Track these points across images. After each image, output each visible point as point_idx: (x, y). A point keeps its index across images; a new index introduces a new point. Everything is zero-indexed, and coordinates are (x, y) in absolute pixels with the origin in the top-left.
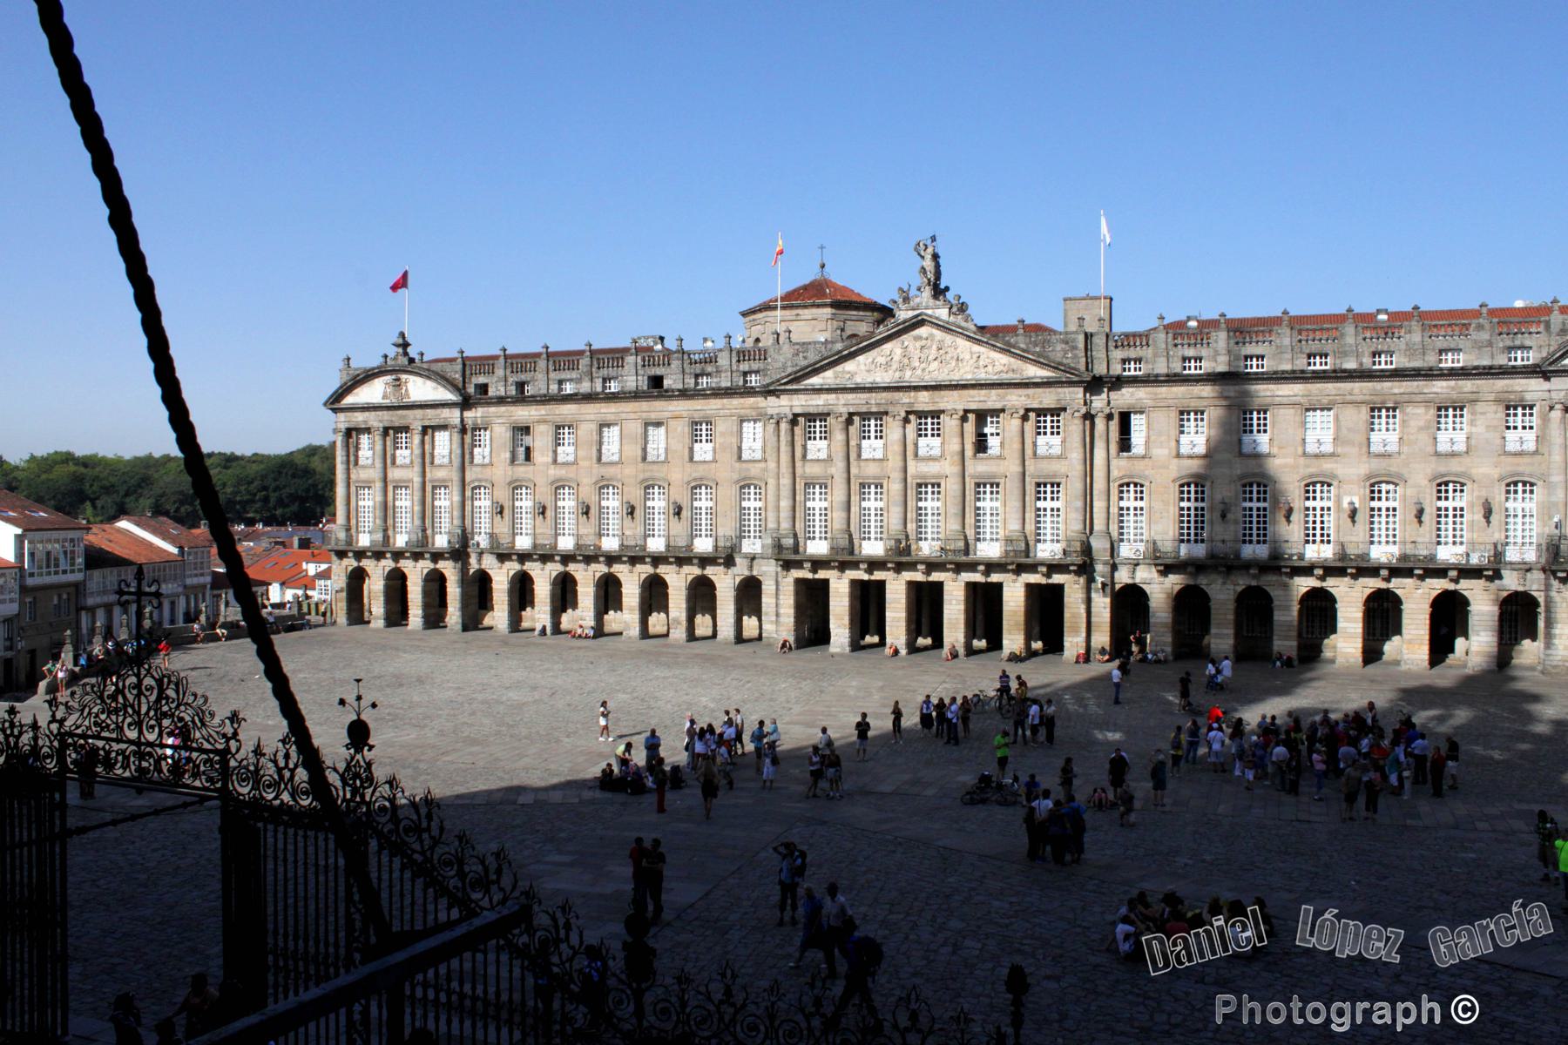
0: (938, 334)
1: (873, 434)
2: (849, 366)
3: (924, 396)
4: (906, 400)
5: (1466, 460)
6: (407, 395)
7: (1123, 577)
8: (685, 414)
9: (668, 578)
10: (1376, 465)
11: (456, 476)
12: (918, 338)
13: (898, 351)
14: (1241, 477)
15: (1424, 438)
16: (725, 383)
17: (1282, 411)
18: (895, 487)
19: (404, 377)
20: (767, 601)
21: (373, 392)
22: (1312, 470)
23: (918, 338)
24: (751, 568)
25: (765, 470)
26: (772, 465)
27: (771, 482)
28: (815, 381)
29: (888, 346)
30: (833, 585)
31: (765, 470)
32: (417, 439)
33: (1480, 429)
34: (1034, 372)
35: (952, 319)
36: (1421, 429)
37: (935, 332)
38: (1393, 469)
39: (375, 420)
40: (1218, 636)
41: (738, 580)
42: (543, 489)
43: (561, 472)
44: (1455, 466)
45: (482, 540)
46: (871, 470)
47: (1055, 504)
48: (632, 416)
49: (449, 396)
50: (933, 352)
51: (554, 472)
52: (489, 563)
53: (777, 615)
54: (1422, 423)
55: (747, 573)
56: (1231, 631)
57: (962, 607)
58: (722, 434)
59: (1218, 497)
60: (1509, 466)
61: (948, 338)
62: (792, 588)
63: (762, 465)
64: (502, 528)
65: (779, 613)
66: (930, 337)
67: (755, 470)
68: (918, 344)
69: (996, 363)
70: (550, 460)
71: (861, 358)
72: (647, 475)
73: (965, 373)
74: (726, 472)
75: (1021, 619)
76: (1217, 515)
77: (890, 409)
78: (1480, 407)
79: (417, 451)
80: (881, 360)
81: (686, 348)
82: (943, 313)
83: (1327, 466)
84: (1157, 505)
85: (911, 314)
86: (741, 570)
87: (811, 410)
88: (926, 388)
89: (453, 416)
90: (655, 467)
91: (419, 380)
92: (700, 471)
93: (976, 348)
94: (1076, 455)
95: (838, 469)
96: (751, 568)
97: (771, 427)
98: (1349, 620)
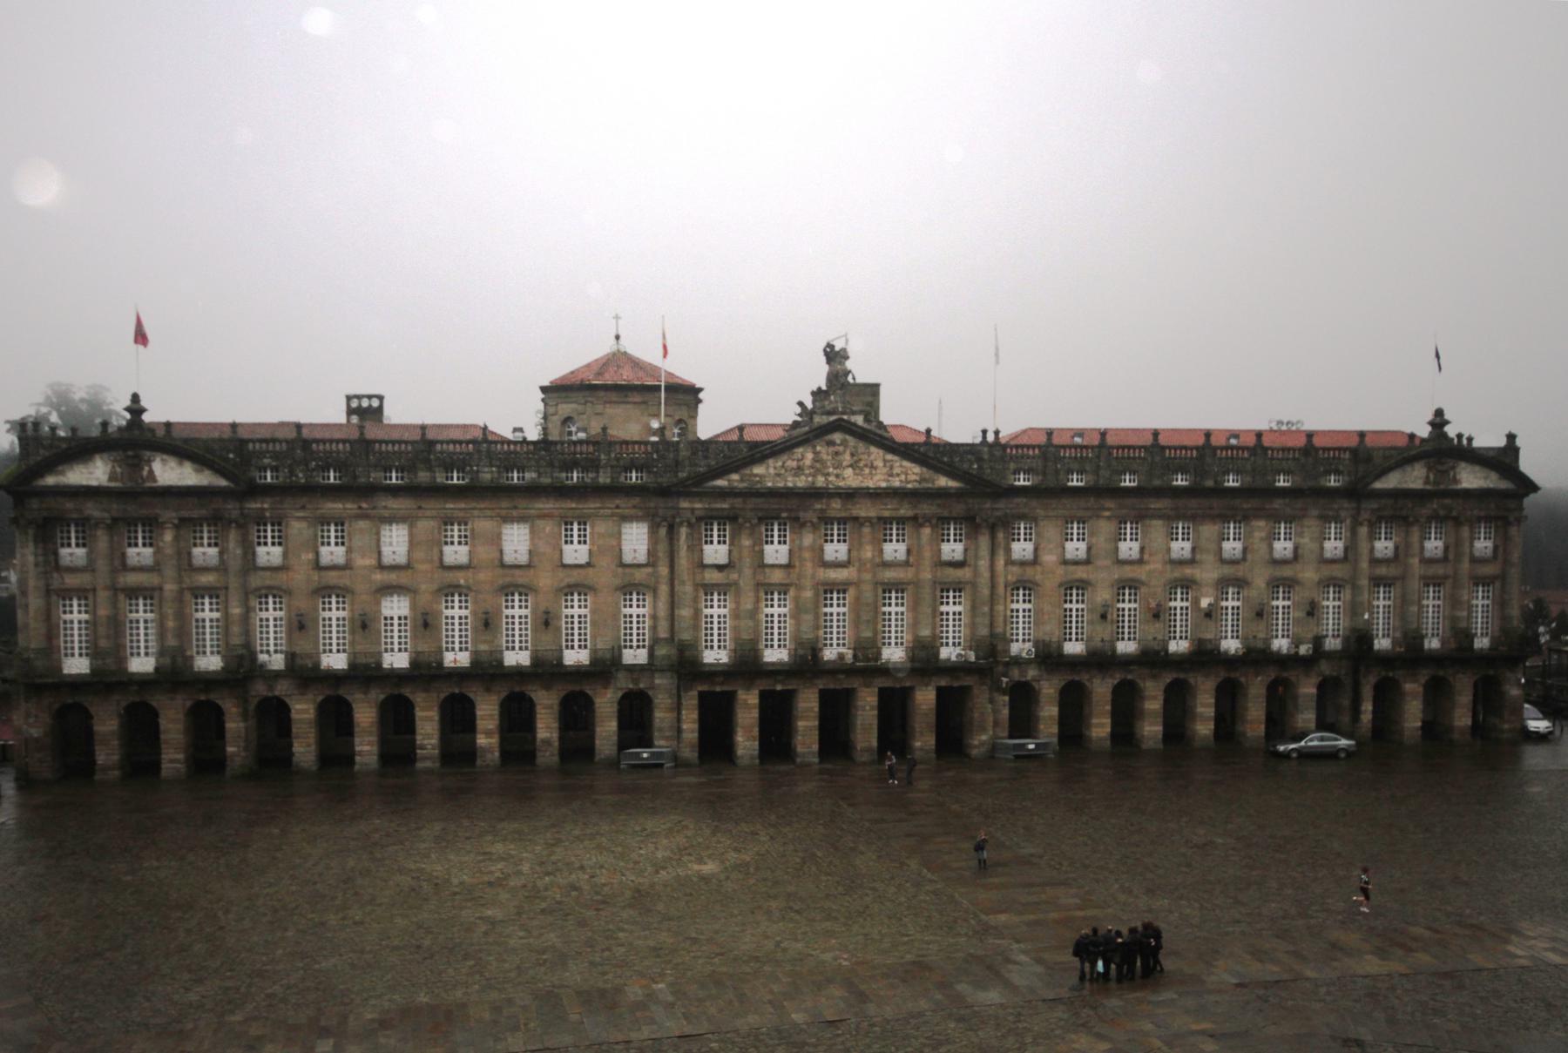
0: (851, 440)
1: (776, 539)
2: (758, 470)
3: (836, 504)
4: (818, 506)
5: (1298, 566)
6: (155, 480)
7: (1016, 674)
8: (556, 512)
9: (533, 695)
10: (1228, 570)
11: (234, 583)
12: (831, 443)
13: (810, 456)
14: (1120, 581)
15: (1263, 547)
16: (604, 479)
17: (1155, 522)
18: (809, 594)
20: (661, 716)
21: (96, 473)
22: (1177, 574)
23: (831, 443)
24: (636, 681)
25: (655, 575)
26: (664, 570)
27: (664, 589)
28: (721, 483)
29: (801, 450)
31: (652, 575)
32: (168, 536)
33: (1305, 540)
34: (943, 482)
35: (866, 426)
36: (1262, 539)
38: (1240, 574)
39: (93, 510)
40: (1099, 725)
41: (620, 694)
42: (364, 597)
43: (392, 577)
44: (1287, 572)
45: (277, 662)
46: (777, 577)
47: (958, 608)
48: (489, 513)
49: (223, 483)
50: (847, 457)
51: (378, 577)
52: (282, 689)
53: (679, 731)
54: (1263, 534)
56: (1109, 721)
59: (1099, 599)
60: (1327, 571)
61: (861, 446)
62: (695, 702)
63: (650, 570)
64: (303, 646)
65: (677, 723)
66: (844, 443)
67: (640, 575)
68: (831, 449)
69: (909, 474)
70: (374, 562)
71: (771, 461)
72: (508, 580)
73: (878, 481)
74: (605, 576)
75: (932, 719)
76: (1097, 617)
77: (801, 514)
78: (1306, 522)
79: (169, 551)
80: (794, 464)
83: (1188, 571)
84: (1047, 608)
85: (825, 420)
86: (624, 683)
88: (839, 495)
89: (231, 508)
90: (517, 572)
91: (172, 462)
92: (575, 576)
93: (889, 457)
94: (983, 564)
95: (746, 578)
96: (636, 681)
97: (663, 531)
98: (1203, 705)
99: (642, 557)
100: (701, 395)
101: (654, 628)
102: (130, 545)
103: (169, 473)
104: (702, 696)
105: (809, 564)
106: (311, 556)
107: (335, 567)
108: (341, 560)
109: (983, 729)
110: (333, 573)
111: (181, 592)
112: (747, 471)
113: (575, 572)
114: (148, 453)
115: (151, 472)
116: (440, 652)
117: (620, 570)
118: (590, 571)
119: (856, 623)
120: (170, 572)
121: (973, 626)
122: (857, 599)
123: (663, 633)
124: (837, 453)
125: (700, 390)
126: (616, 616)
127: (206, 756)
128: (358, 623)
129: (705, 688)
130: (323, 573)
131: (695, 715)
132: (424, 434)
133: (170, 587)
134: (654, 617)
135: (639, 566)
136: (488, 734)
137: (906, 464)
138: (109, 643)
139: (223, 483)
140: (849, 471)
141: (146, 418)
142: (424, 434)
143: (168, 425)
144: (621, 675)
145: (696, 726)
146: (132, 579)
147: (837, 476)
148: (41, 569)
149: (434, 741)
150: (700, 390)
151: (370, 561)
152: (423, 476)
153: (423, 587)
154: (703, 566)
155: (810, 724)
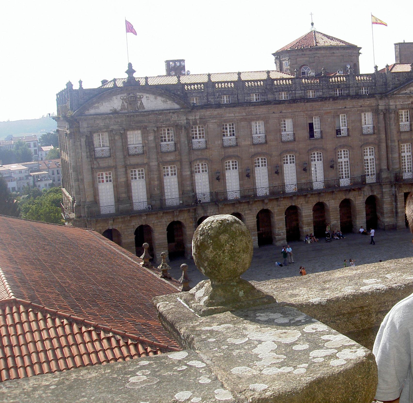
6: (144, 108)
9: (327, 203)
19: (139, 94)
24: (372, 191)
26: (383, 136)
27: (384, 145)
49: (177, 106)
51: (253, 150)
55: (371, 194)
63: (375, 136)
86: (367, 192)
87: (405, 106)
91: (152, 97)
97: (381, 116)
100: (360, 51)
101: (379, 165)
102: (162, 141)
103: (150, 103)
106: (220, 142)
107: (230, 147)
108: (233, 143)
110: (231, 150)
111: (159, 164)
113: (343, 140)
114: (140, 94)
115: (142, 104)
116: (311, 183)
117: (362, 137)
118: (350, 138)
120: (154, 156)
123: (384, 167)
125: (360, 48)
127: (294, 235)
128: (245, 175)
130: (227, 150)
132: (209, 79)
133: (154, 164)
134: (379, 159)
136: (309, 224)
138: (123, 194)
139: (177, 106)
141: (135, 75)
142: (239, 77)
143: (146, 78)
144: (366, 188)
146: (133, 161)
148: (89, 160)
149: (284, 231)
150: (360, 48)
151: (248, 143)
152: (270, 97)
153: (274, 153)
154: (401, 132)
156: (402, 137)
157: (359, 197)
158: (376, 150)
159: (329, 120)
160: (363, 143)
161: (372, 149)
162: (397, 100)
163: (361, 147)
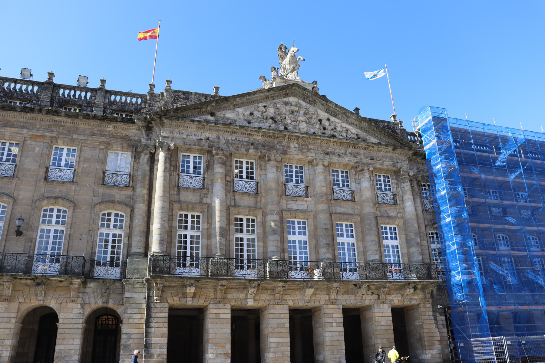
12: (286, 103)
23: (286, 103)
27: (141, 207)
30: (212, 311)
34: (373, 140)
37: (301, 102)
41: (88, 311)
53: (147, 346)
55: (100, 303)
57: (342, 329)
58: (86, 160)
61: (311, 109)
63: (129, 192)
68: (288, 108)
71: (240, 110)
81: (56, 81)
82: (310, 88)
93: (332, 119)
97: (145, 158)
99: (123, 179)
104: (172, 310)
105: (274, 193)
109: (431, 346)
112: (220, 114)
117: (101, 190)
118: (73, 187)
119: (316, 247)
121: (409, 255)
122: (316, 228)
124: (292, 112)
126: (92, 232)
129: (176, 301)
131: (165, 330)
134: (130, 235)
135: (120, 187)
137: (344, 125)
140: (304, 124)
145: (165, 341)
147: (295, 126)
155: (282, 340)
156: (182, 198)
157: (69, 305)
158: (129, 218)
159: (37, 149)
160: (100, 201)
161: (122, 216)
162: (177, 131)
163: (96, 205)
